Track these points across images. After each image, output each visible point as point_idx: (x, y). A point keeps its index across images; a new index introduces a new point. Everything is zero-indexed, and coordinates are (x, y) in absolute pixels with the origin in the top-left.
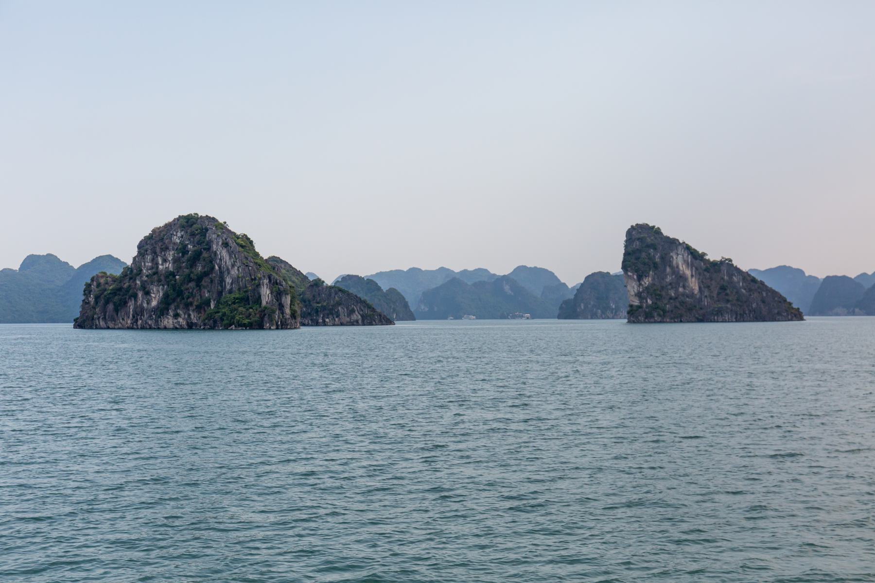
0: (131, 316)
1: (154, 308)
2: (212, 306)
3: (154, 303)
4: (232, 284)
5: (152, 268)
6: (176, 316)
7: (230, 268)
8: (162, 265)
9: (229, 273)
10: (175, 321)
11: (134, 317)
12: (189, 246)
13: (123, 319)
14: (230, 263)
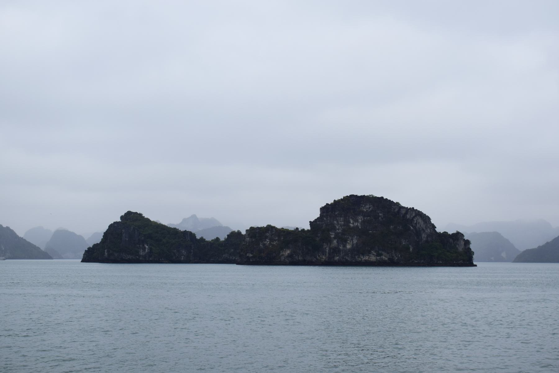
0: (327, 254)
1: (349, 250)
2: (411, 250)
3: (349, 246)
4: (427, 237)
5: (344, 225)
6: (379, 255)
7: (424, 228)
8: (353, 224)
9: (424, 231)
10: (378, 258)
11: (329, 254)
12: (380, 214)
13: (319, 256)
14: (424, 226)
